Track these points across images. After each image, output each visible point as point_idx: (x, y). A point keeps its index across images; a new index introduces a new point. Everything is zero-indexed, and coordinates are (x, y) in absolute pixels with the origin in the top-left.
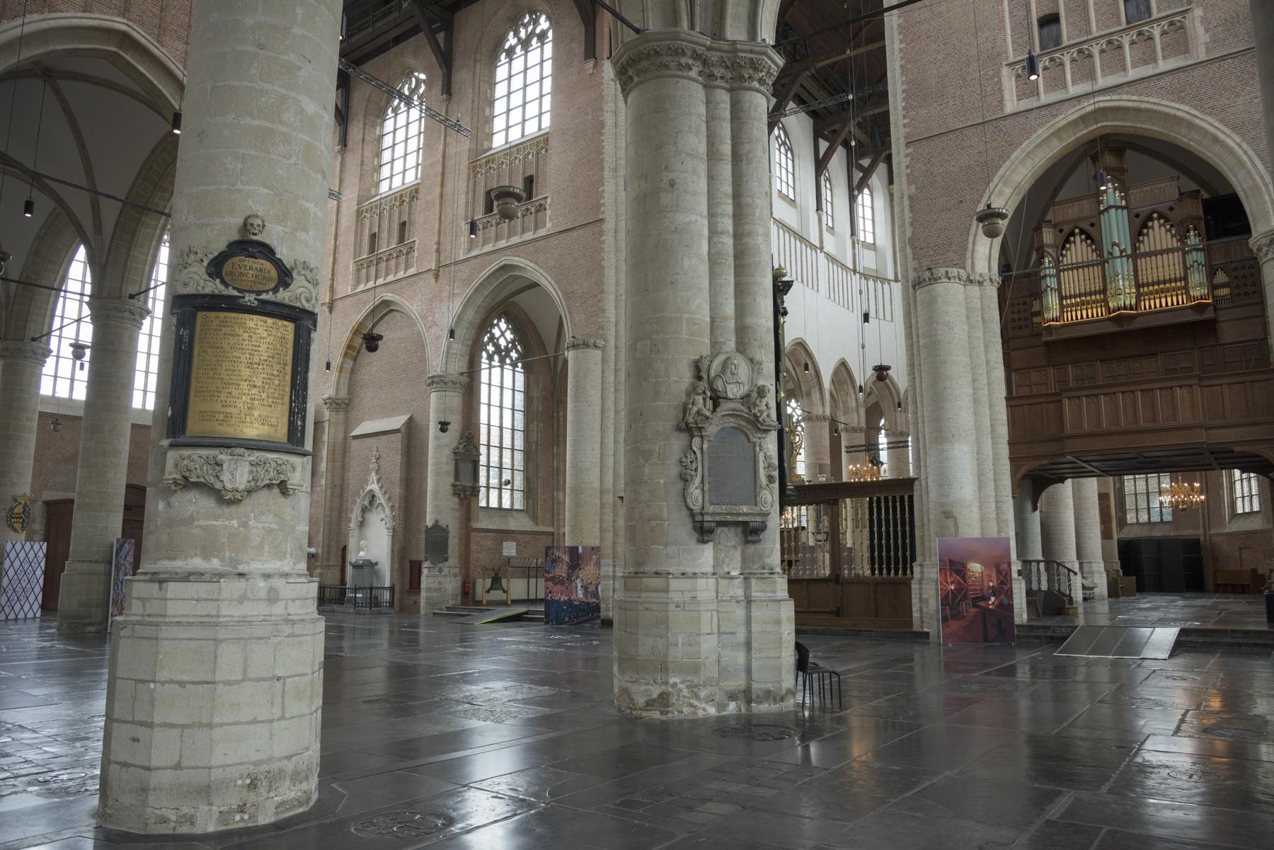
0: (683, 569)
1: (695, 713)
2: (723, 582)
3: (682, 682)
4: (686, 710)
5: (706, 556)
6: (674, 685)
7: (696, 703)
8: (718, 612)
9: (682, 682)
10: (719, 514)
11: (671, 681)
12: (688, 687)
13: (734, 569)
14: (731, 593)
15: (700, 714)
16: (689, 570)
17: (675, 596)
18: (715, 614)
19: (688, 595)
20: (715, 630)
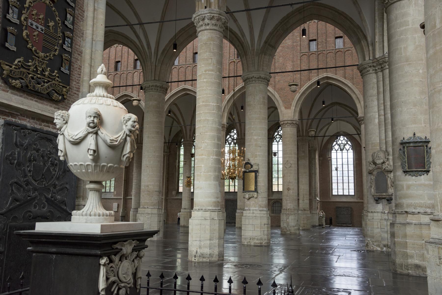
0: (372, 210)
1: (373, 249)
2: (383, 214)
3: (371, 240)
4: (372, 248)
5: (380, 207)
6: (369, 241)
7: (374, 246)
8: (380, 222)
9: (371, 240)
10: (378, 196)
11: (368, 240)
12: (372, 242)
13: (386, 211)
14: (385, 217)
15: (375, 249)
16: (373, 211)
17: (369, 218)
18: (379, 223)
19: (372, 217)
20: (379, 227)
